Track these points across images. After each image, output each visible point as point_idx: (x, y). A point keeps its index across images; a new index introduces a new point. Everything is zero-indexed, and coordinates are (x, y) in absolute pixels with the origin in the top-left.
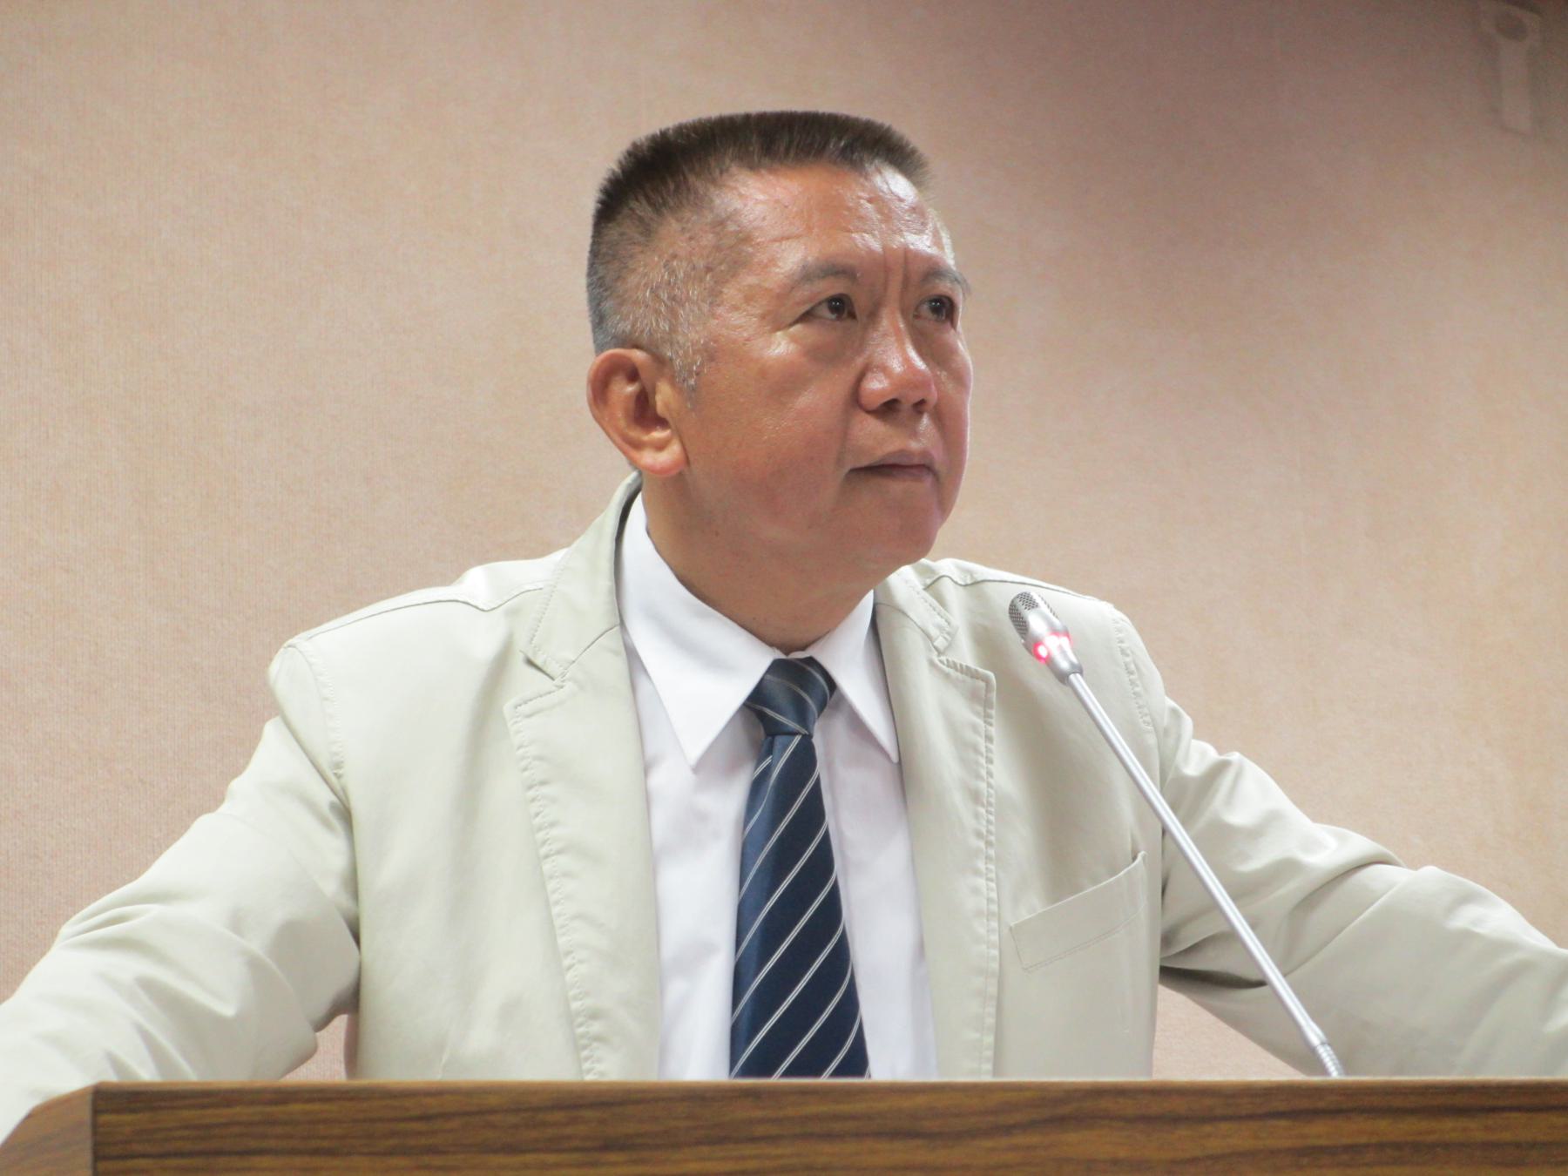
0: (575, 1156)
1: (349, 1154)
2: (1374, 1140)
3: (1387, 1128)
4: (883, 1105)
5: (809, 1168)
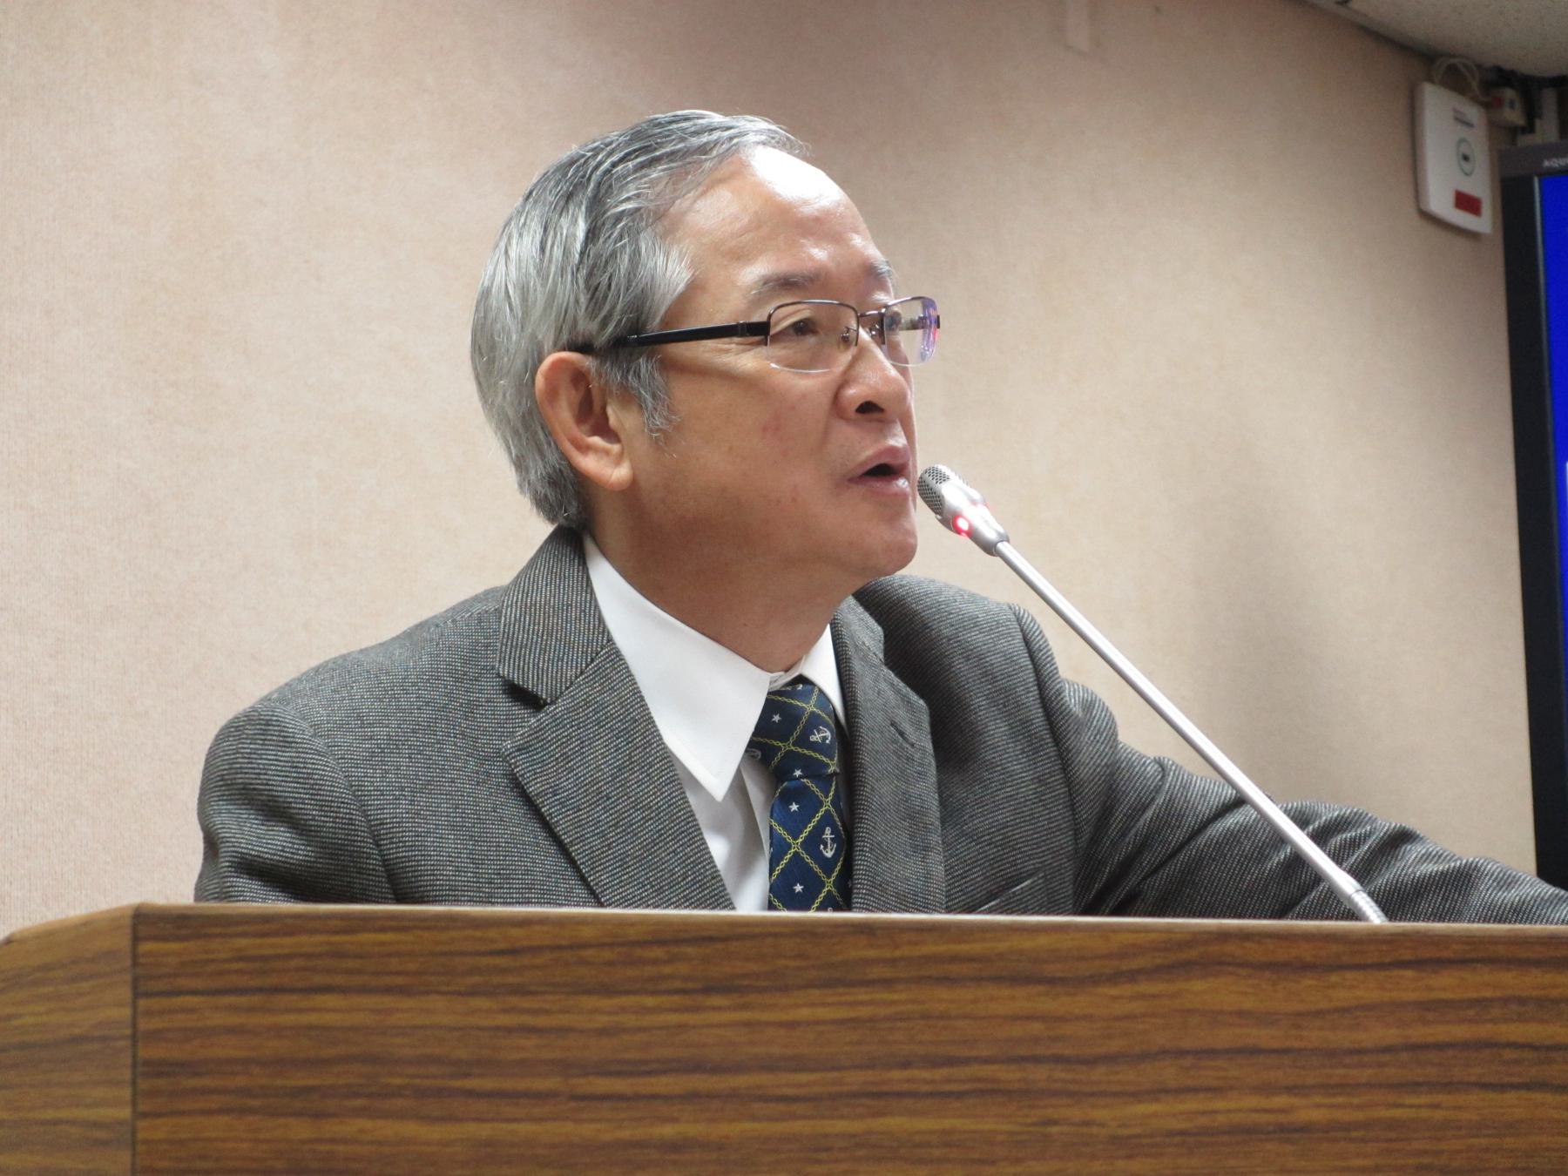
0: (676, 999)
1: (427, 993)
2: (1498, 994)
3: (1510, 981)
4: (1003, 946)
5: (926, 1016)
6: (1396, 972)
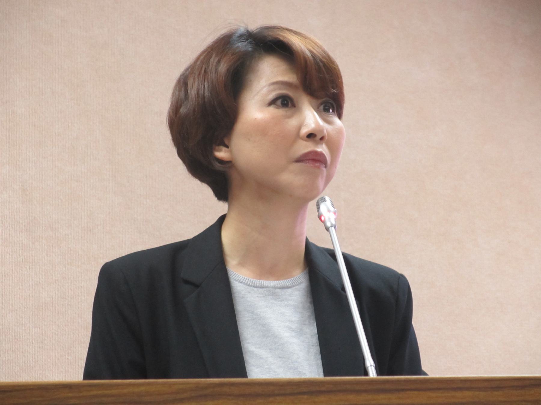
4: (125, 391)
6: (301, 396)
